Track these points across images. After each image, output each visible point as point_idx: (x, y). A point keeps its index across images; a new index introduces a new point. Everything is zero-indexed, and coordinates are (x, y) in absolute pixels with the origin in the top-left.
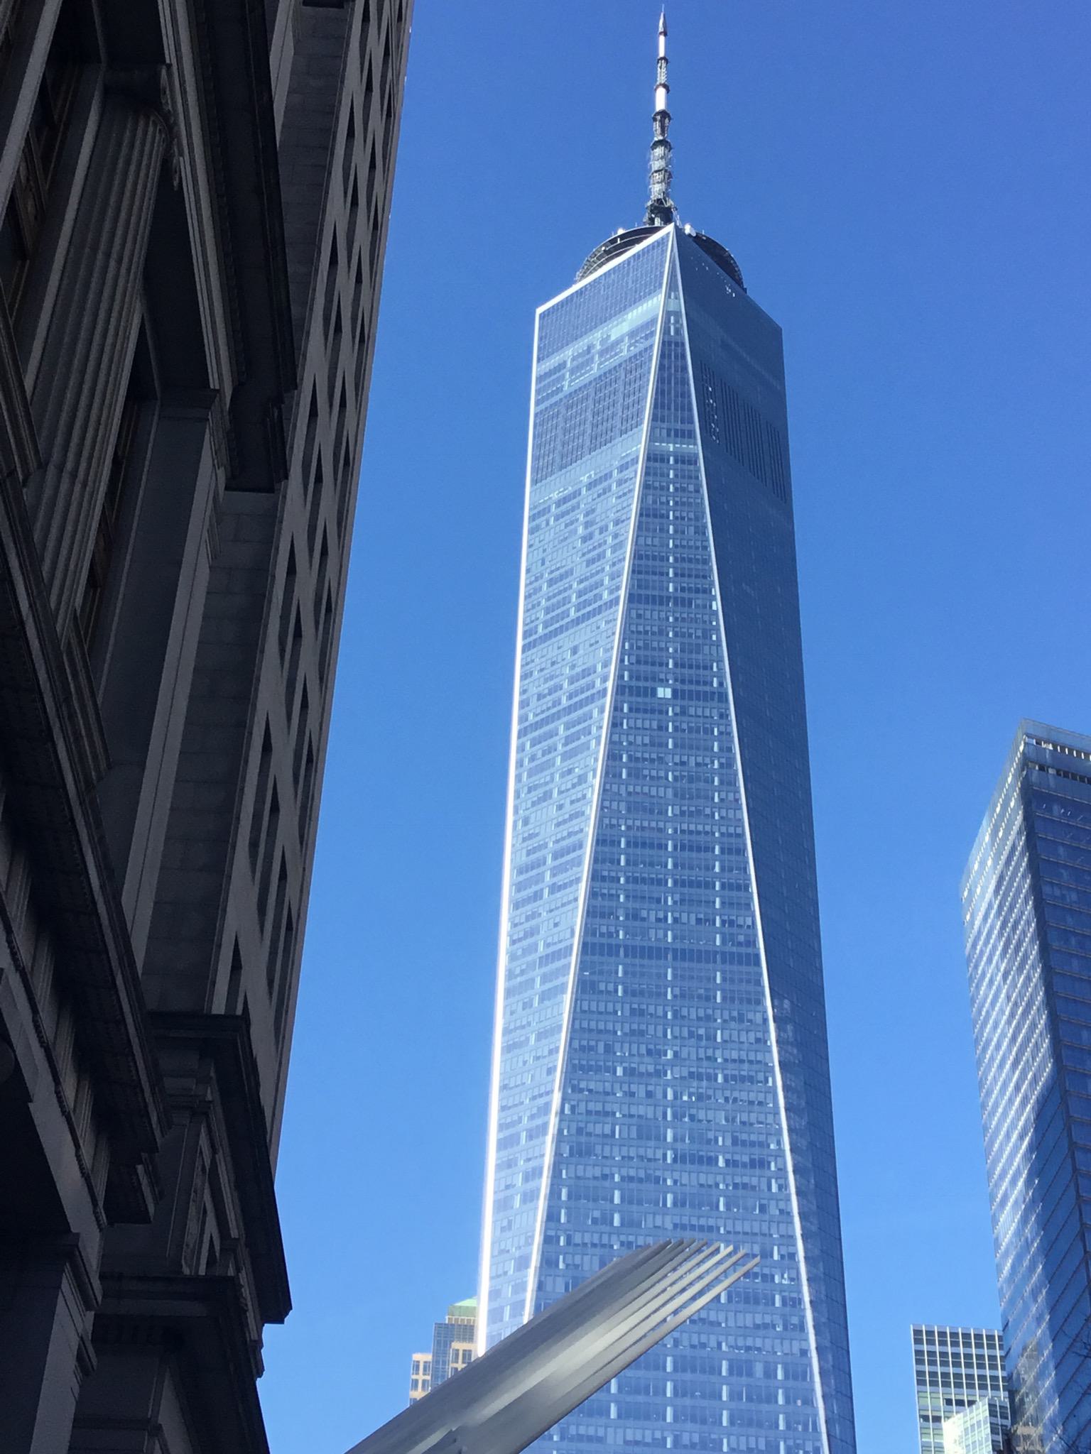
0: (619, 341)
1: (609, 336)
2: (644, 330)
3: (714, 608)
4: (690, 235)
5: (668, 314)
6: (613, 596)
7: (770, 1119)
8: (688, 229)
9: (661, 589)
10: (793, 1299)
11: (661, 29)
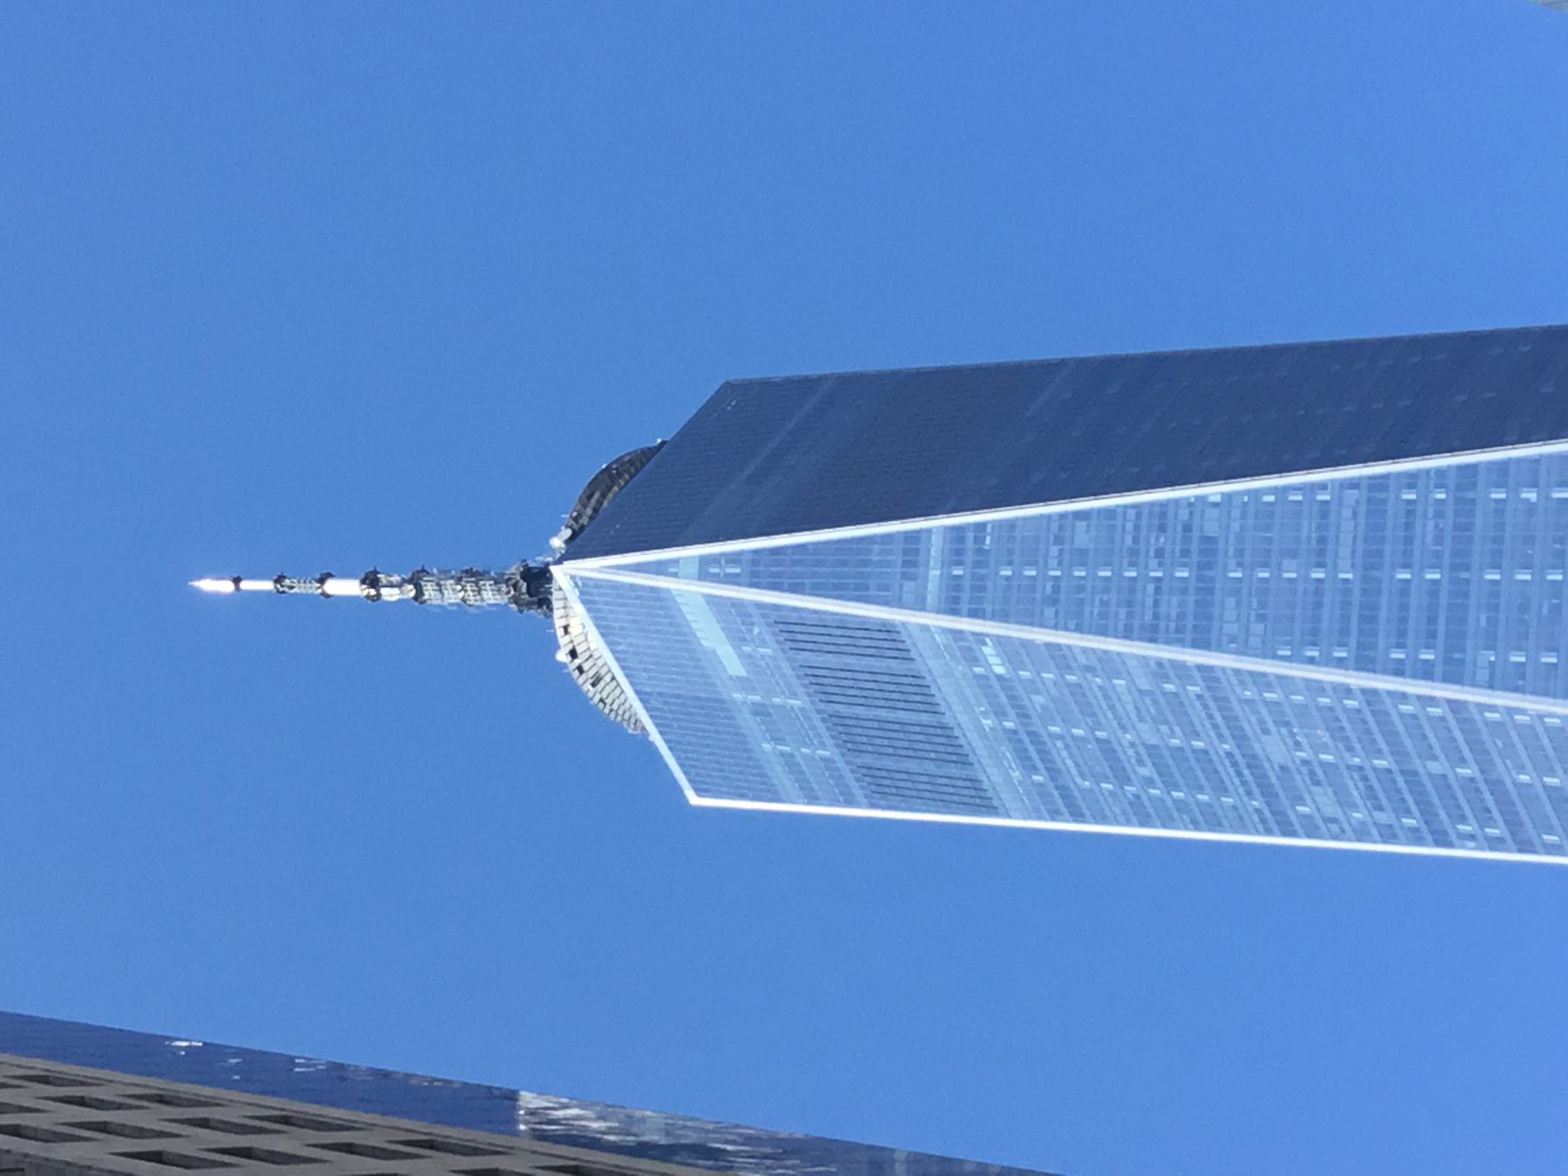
0: (747, 659)
1: (740, 679)
2: (734, 617)
3: (1218, 499)
4: (568, 541)
6: (1196, 675)
8: (557, 542)
9: (1184, 591)
11: (226, 587)
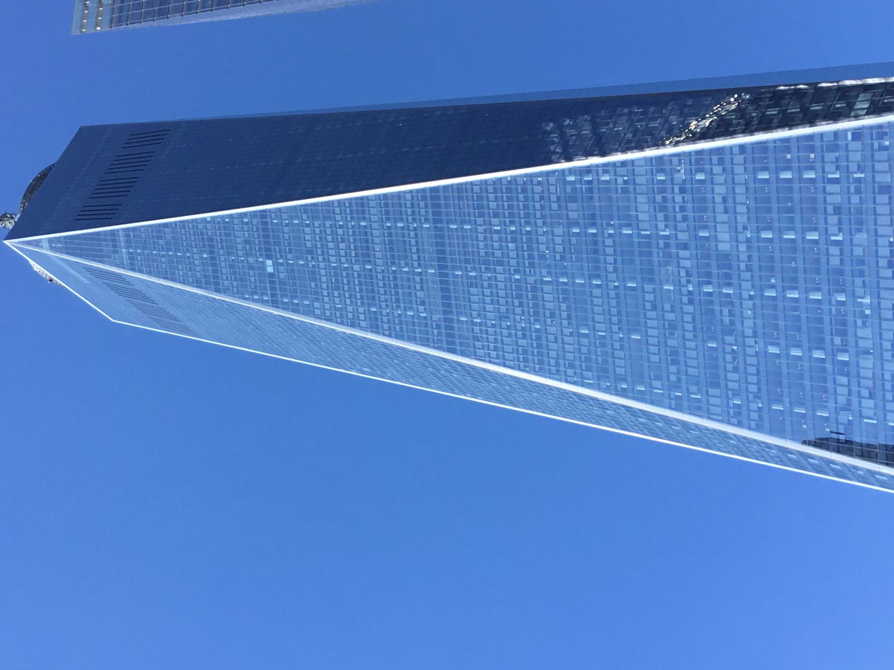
0: (88, 279)
3: (209, 219)
5: (51, 248)
7: (552, 180)
10: (698, 161)
